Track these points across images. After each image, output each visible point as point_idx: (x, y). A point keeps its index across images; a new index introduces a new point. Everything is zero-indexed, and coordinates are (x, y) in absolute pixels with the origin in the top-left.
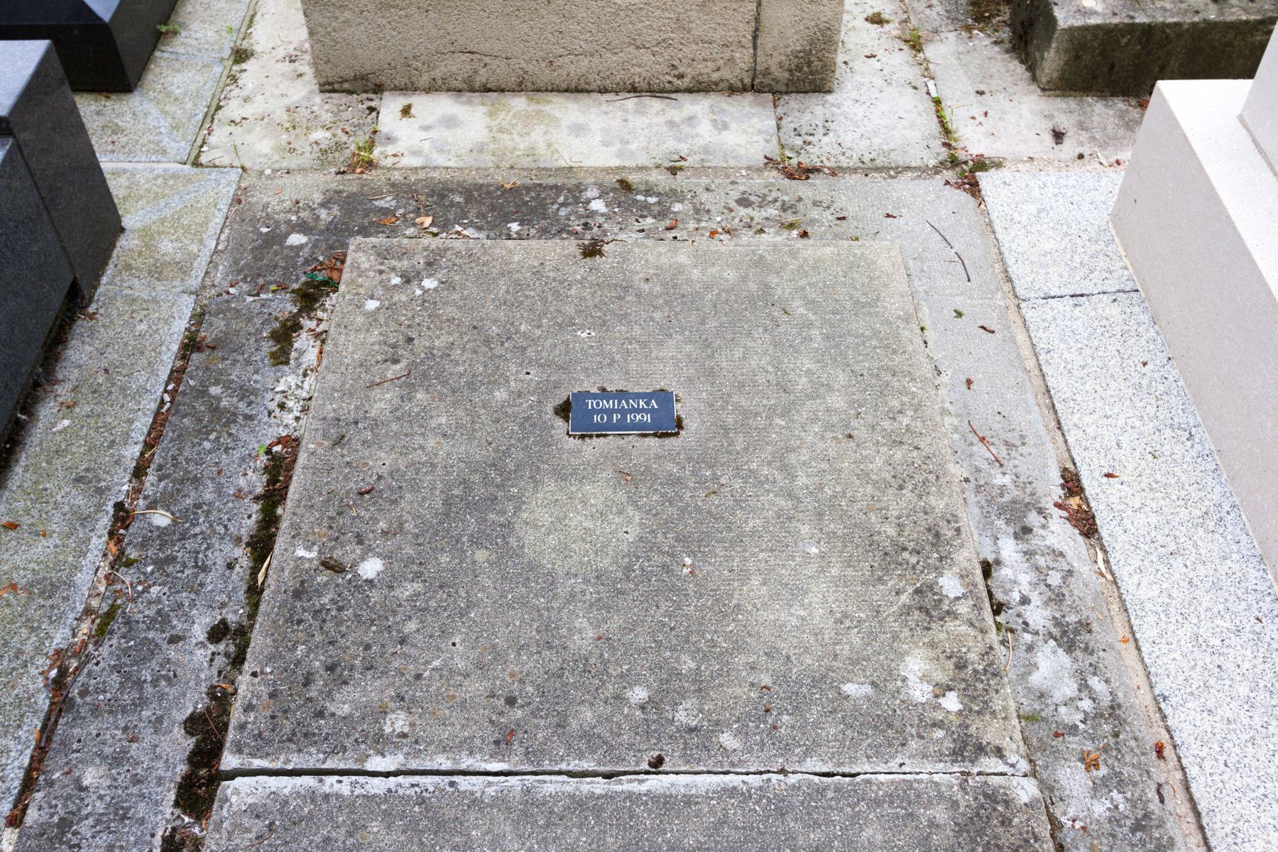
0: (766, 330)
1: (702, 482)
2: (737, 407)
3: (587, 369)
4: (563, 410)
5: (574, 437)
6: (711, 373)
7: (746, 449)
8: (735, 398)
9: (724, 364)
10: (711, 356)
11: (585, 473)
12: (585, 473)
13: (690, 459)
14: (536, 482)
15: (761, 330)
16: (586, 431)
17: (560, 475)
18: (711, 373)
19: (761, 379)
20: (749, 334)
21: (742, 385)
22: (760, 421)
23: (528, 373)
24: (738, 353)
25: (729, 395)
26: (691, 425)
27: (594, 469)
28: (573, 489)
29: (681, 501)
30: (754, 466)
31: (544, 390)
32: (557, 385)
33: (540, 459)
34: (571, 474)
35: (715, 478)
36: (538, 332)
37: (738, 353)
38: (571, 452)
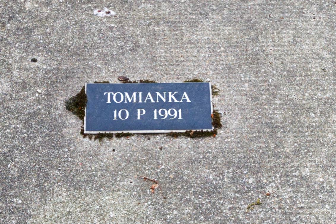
0: (321, 8)
1: (244, 191)
2: (286, 101)
3: (105, 55)
4: (77, 105)
5: (90, 136)
6: (254, 60)
7: (297, 152)
8: (284, 90)
9: (270, 49)
10: (255, 40)
11: (103, 180)
12: (103, 180)
13: (229, 164)
14: (44, 191)
15: (314, 8)
16: (105, 129)
17: (72, 182)
18: (254, 60)
19: (315, 67)
20: (301, 13)
21: (292, 74)
22: (315, 118)
23: (34, 60)
24: (287, 36)
25: (277, 87)
26: (231, 122)
27: (114, 175)
28: (89, 199)
29: (219, 214)
30: (306, 172)
31: (53, 80)
32: (69, 75)
33: (49, 163)
34: (86, 182)
35: (260, 186)
36: (46, 11)
37: (287, 36)
38: (86, 155)
